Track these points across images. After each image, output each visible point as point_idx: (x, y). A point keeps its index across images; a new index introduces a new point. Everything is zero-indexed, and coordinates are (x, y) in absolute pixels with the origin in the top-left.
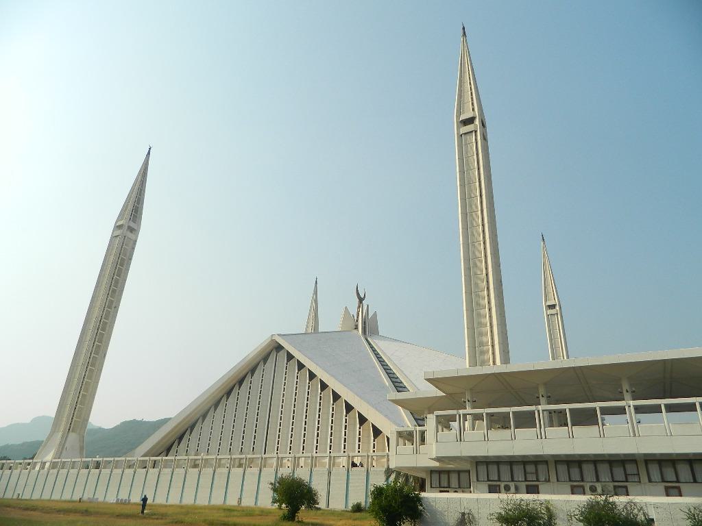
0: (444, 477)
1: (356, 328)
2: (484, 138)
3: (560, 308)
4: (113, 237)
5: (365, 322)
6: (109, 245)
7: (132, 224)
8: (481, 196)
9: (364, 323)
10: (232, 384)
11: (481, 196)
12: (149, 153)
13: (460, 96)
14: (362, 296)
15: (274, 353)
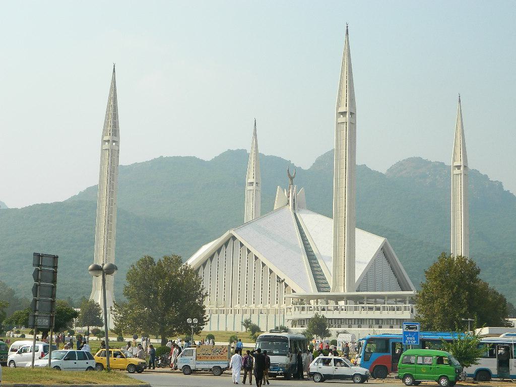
0: (302, 321)
1: (288, 203)
2: (353, 124)
3: (465, 167)
4: (102, 150)
5: (294, 201)
6: (101, 157)
7: (115, 139)
8: (346, 168)
9: (294, 201)
10: (206, 259)
11: (346, 168)
12: (114, 71)
13: (340, 90)
14: (292, 175)
15: (231, 241)
